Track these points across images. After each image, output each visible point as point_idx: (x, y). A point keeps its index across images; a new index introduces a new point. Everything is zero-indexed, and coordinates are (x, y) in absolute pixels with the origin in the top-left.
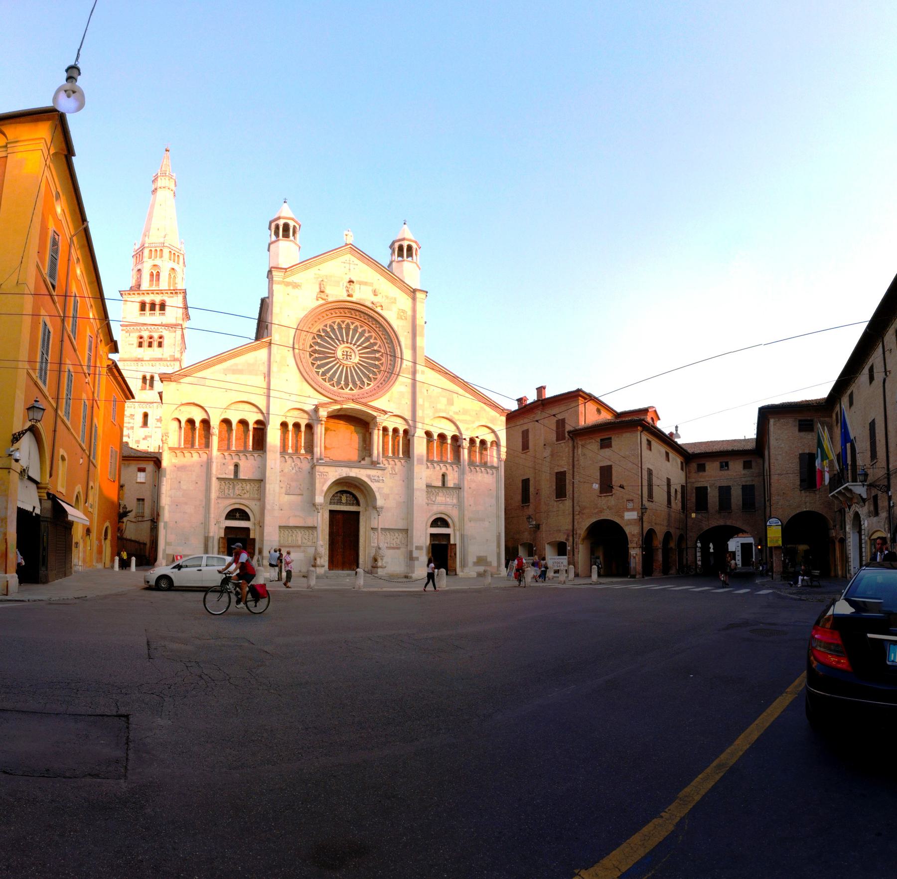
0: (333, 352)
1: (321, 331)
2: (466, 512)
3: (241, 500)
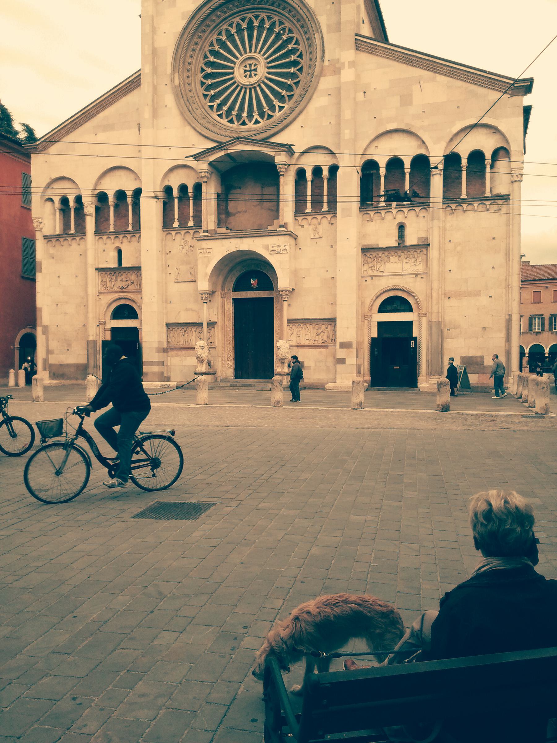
0: (231, 71)
1: (215, 43)
2: (435, 285)
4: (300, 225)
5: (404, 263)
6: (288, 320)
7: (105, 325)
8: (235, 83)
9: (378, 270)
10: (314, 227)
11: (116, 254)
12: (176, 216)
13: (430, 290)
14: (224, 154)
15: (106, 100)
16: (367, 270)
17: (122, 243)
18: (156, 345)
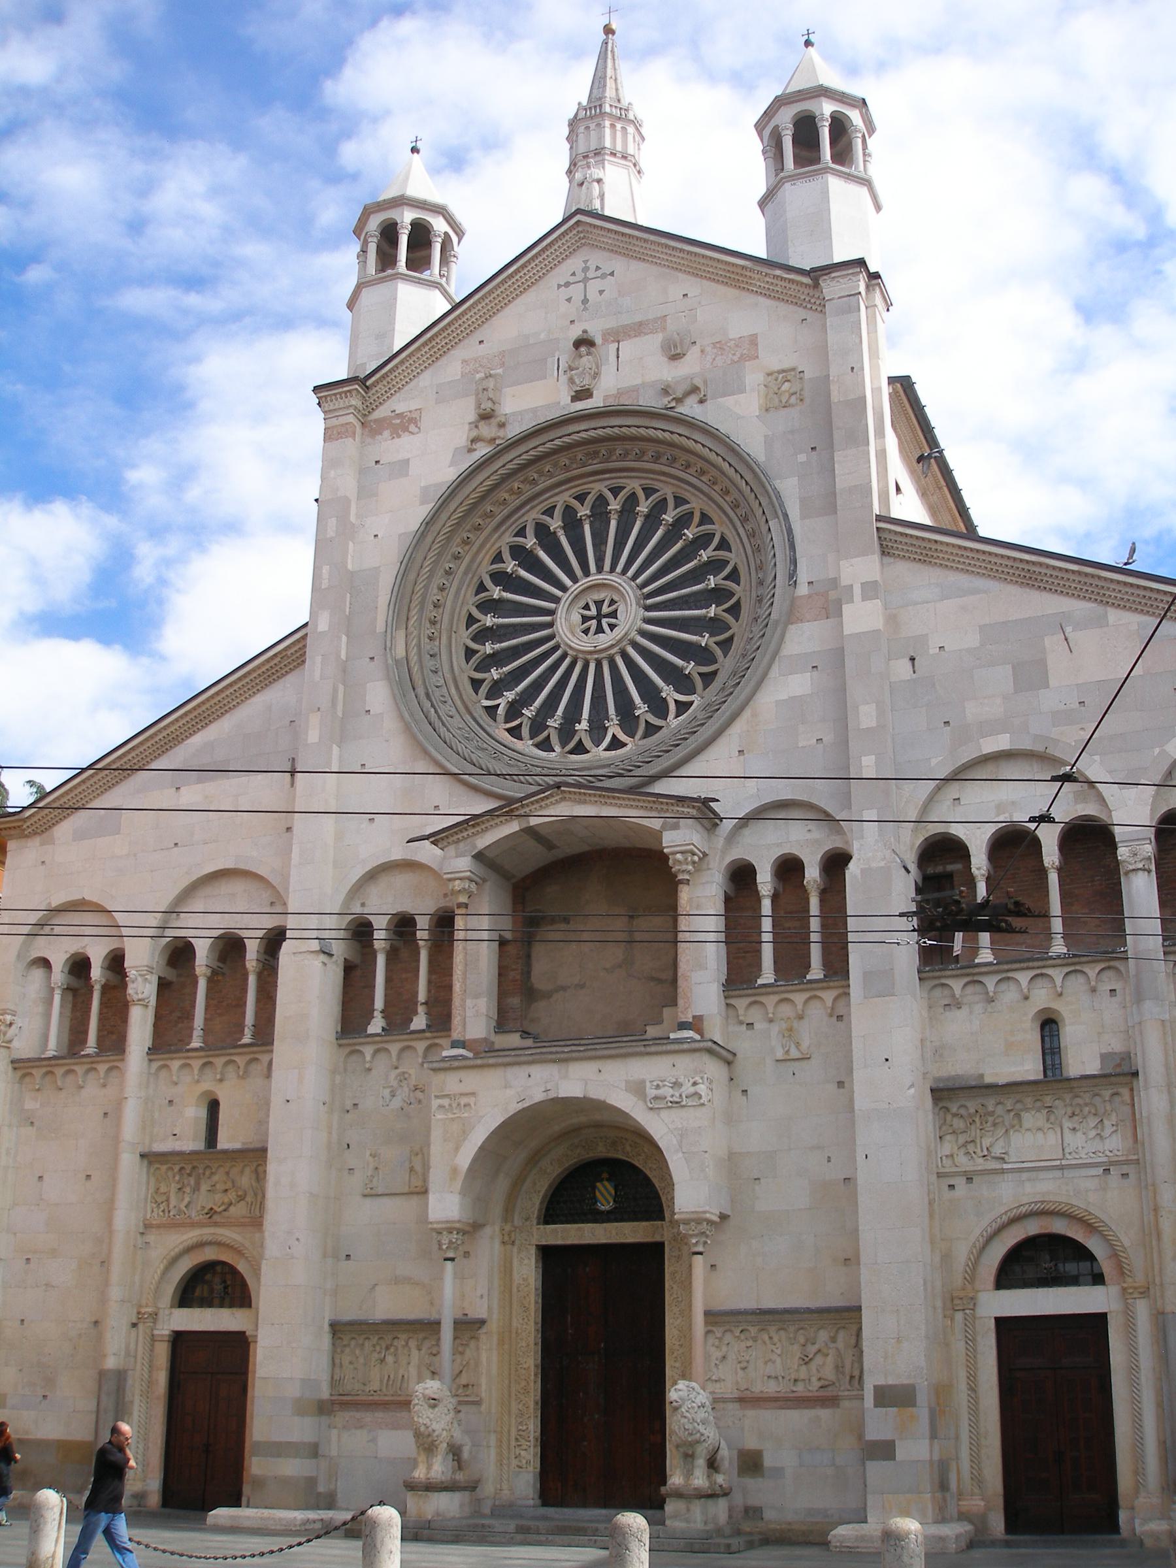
1: (506, 555)
4: (741, 1023)
5: (1066, 1131)
6: (707, 1314)
7: (155, 1323)
8: (556, 648)
9: (986, 1153)
10: (784, 1025)
11: (203, 1113)
12: (379, 1003)
14: (517, 828)
15: (212, 702)
16: (952, 1156)
17: (221, 1080)
18: (293, 1391)
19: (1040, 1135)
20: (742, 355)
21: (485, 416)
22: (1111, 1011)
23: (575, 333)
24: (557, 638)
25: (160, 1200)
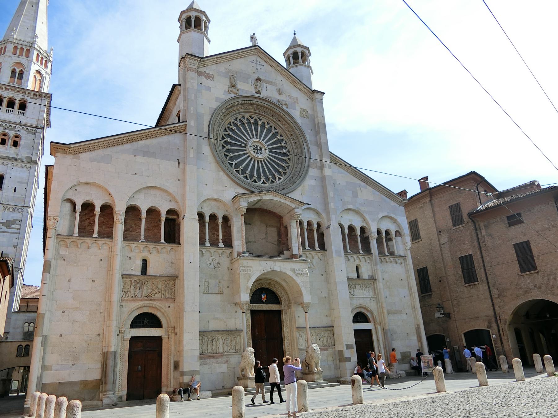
2: (384, 305)
3: (152, 302)
8: (247, 153)
13: (381, 309)
19: (359, 290)
20: (295, 101)
21: (233, 86)
22: (369, 266)
23: (256, 76)
24: (247, 151)
25: (126, 291)
